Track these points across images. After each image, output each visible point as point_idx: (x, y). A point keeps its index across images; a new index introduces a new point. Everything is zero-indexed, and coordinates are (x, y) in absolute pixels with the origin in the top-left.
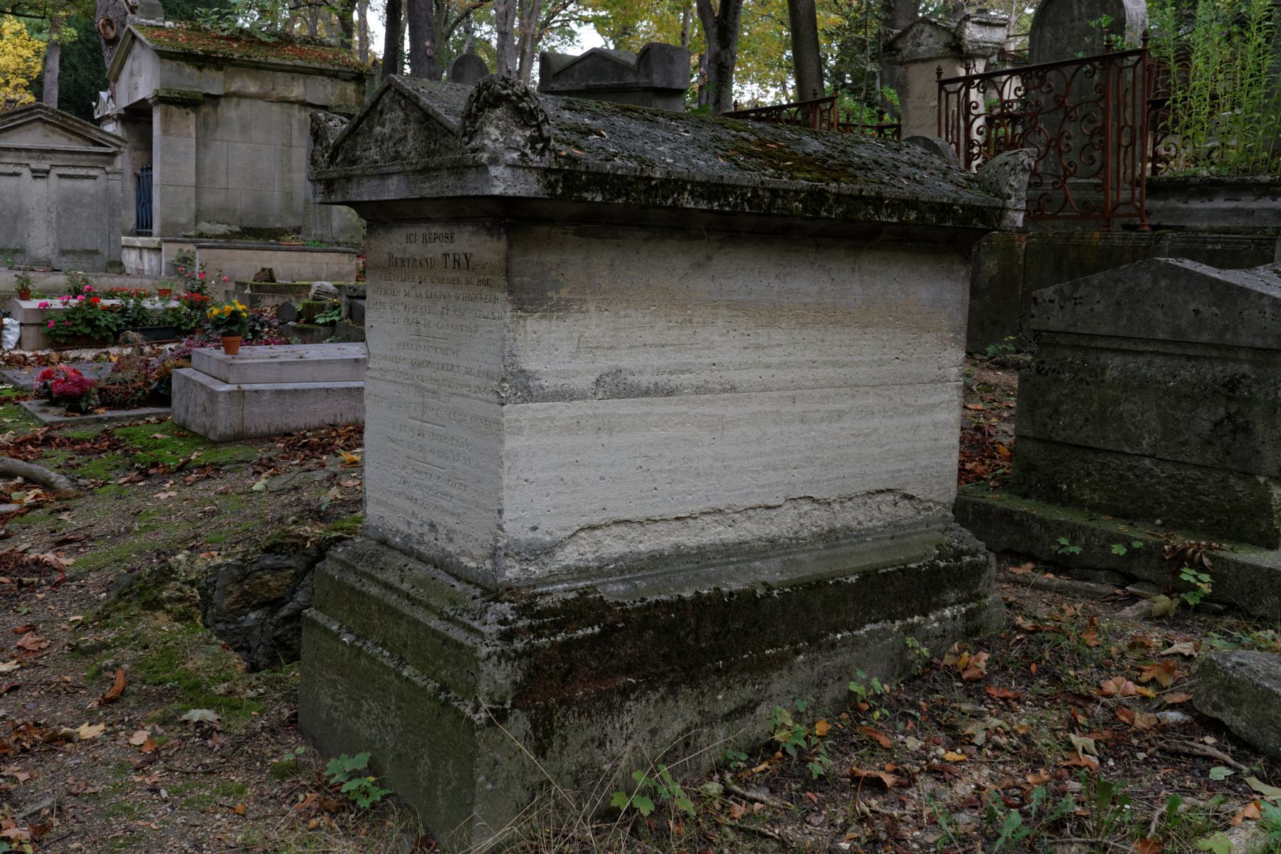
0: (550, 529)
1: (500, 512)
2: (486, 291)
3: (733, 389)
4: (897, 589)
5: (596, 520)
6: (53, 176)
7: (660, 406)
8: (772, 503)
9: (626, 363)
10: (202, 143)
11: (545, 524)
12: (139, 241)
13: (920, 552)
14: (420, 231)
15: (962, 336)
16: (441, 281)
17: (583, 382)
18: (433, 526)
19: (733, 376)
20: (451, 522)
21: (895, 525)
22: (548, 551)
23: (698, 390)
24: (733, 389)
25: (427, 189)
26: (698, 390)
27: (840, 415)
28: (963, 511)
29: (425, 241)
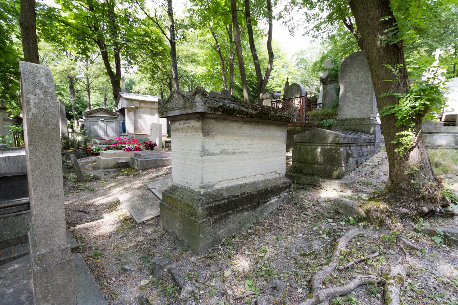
0: (212, 181)
1: (202, 179)
2: (197, 133)
3: (246, 153)
4: (275, 191)
5: (221, 180)
6: (105, 121)
7: (233, 156)
8: (254, 175)
9: (226, 148)
10: (134, 114)
11: (193, 185)
12: (123, 134)
13: (280, 183)
14: (182, 122)
15: (286, 143)
16: (187, 132)
17: (218, 152)
18: (187, 183)
19: (246, 150)
20: (191, 182)
21: (275, 178)
22: (212, 186)
23: (240, 153)
24: (246, 153)
25: (185, 112)
26: (240, 153)
27: (265, 157)
28: (286, 175)
29: (184, 124)
